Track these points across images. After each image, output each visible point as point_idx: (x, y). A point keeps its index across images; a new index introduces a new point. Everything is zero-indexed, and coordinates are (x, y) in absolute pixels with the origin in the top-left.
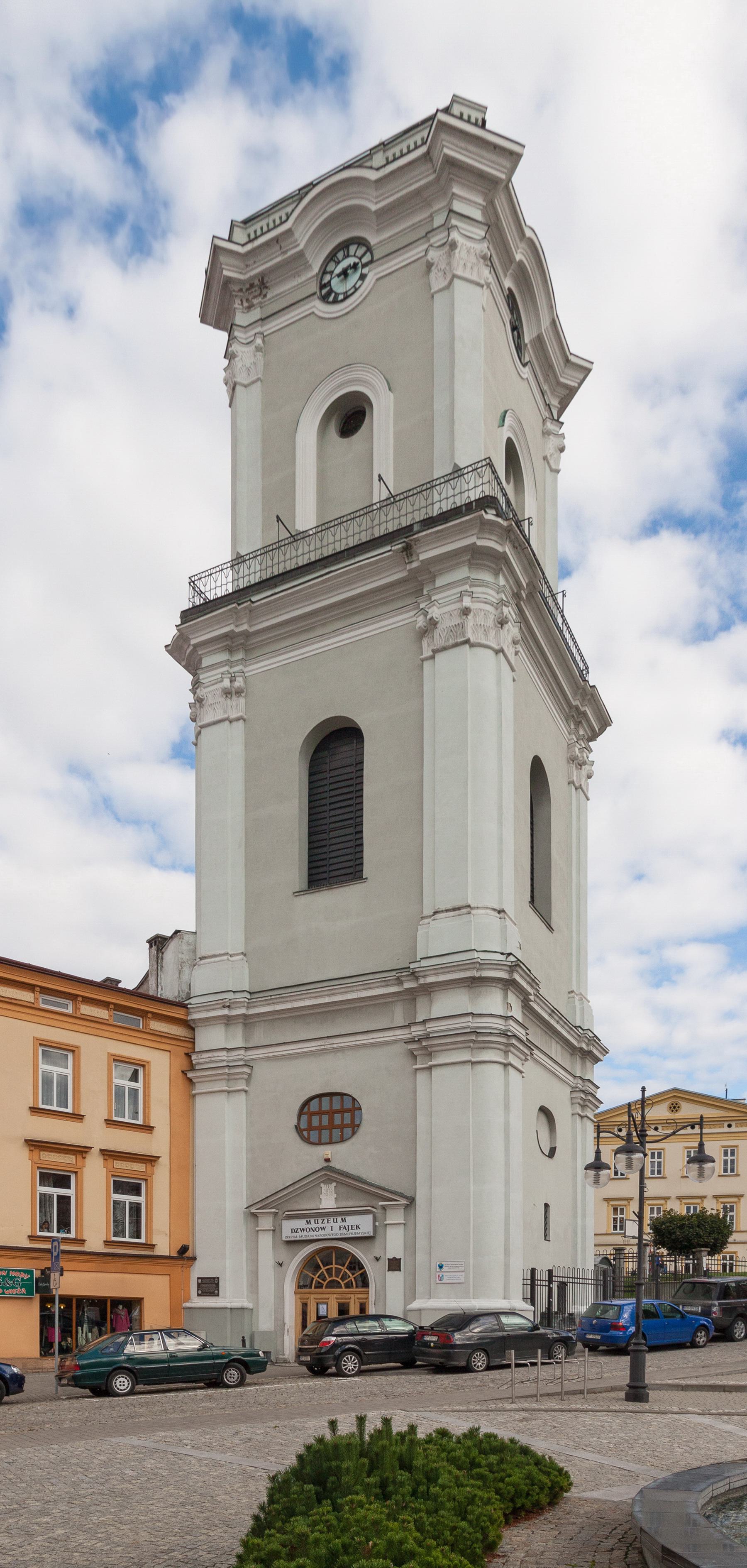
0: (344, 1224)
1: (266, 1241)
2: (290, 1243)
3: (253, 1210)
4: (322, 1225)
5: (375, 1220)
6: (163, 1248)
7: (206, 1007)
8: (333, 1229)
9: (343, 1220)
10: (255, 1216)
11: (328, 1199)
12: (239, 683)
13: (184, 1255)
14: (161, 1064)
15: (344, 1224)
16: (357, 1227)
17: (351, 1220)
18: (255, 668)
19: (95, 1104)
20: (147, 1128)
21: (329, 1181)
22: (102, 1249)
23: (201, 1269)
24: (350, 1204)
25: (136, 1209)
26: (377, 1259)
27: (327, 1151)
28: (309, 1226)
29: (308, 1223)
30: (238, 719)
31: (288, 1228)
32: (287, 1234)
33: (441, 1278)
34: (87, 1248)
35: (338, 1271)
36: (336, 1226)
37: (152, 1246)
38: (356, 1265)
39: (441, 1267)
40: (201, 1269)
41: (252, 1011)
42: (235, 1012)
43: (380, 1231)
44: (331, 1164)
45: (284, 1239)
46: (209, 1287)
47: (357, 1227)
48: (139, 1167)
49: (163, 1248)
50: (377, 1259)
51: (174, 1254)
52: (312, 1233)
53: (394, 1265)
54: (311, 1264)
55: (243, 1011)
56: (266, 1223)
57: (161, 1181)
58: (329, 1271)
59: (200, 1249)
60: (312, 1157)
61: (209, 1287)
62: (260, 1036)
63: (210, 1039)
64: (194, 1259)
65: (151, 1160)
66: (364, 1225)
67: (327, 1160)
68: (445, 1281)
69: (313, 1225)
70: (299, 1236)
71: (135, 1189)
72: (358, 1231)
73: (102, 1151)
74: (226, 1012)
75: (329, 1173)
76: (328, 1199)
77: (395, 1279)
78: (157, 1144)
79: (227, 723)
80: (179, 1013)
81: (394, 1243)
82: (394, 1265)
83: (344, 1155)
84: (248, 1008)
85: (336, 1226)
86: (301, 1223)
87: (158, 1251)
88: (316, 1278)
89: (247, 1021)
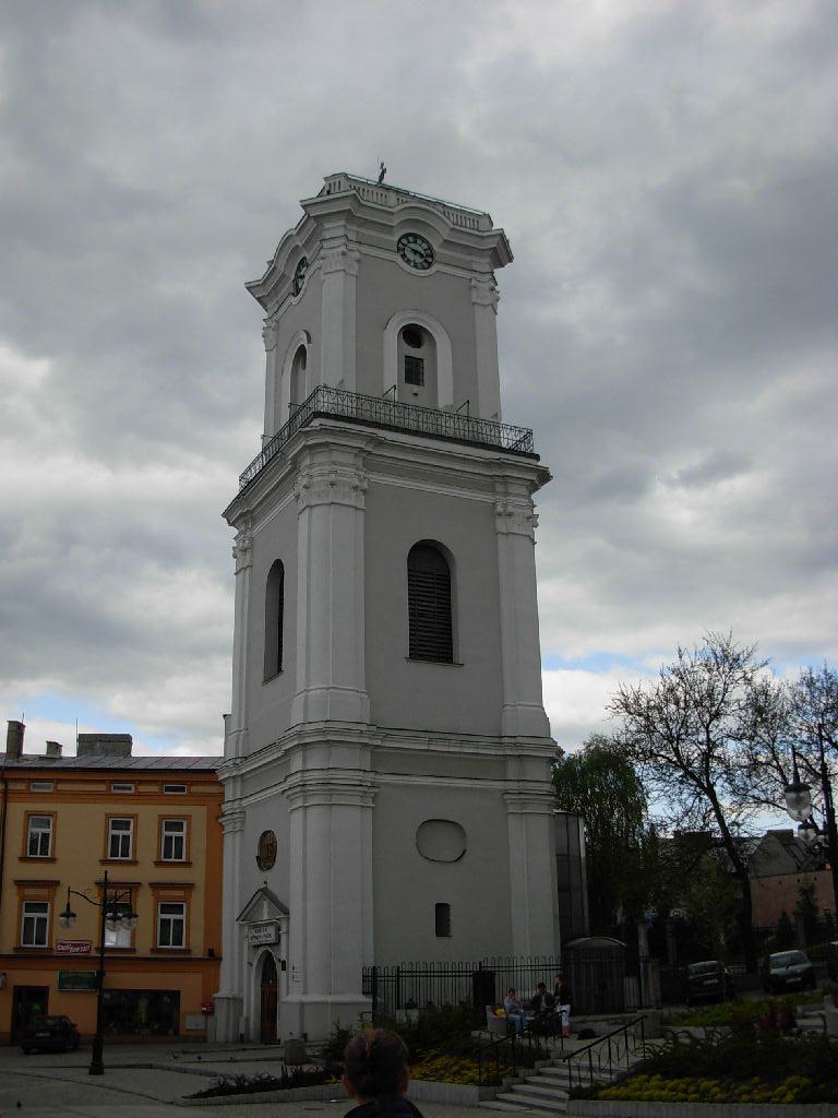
6: (198, 950)
22: (149, 955)
34: (137, 955)
48: (180, 893)
49: (198, 950)
57: (198, 900)
63: (229, 796)
64: (221, 959)
65: (188, 887)
71: (178, 909)
73: (151, 885)
78: (196, 875)
80: (208, 777)
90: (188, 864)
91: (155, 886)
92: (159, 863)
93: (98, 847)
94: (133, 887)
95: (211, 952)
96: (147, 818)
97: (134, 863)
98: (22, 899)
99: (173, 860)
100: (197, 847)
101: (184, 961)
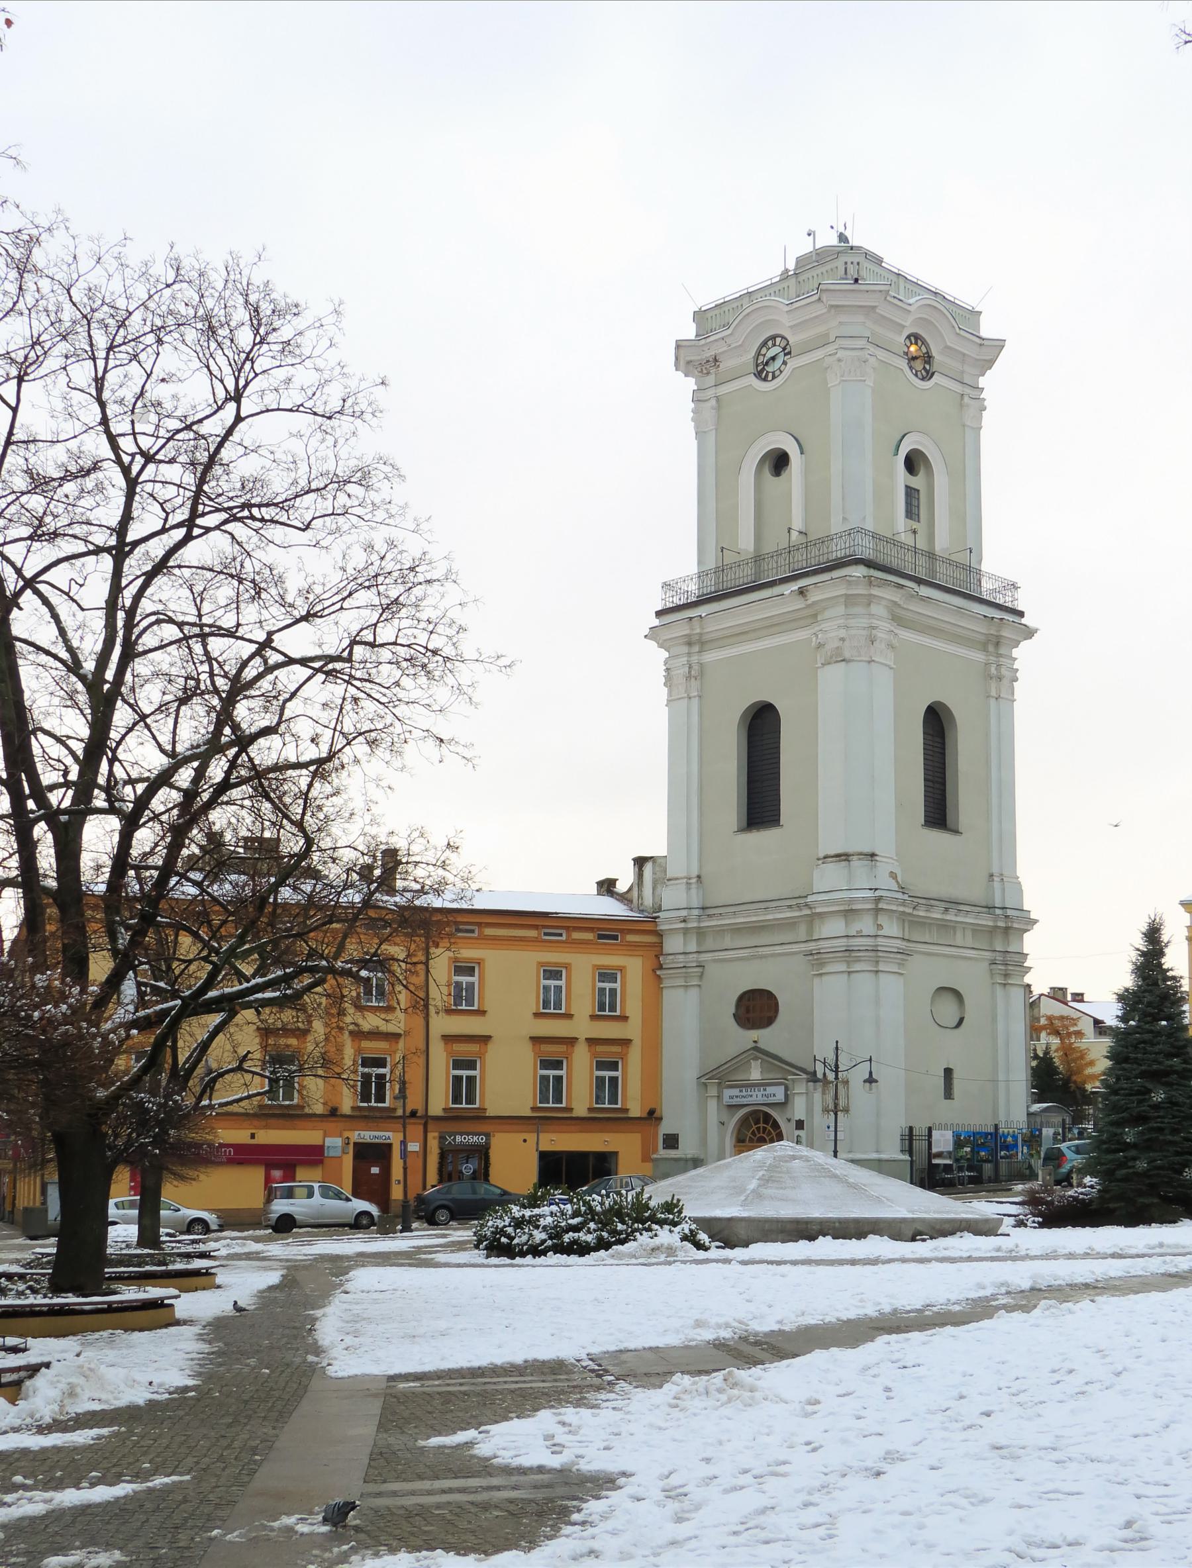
1: (712, 1105)
2: (730, 1106)
3: (703, 1080)
5: (787, 1089)
6: (636, 1111)
7: (669, 920)
8: (757, 1097)
10: (705, 1084)
11: (755, 1073)
13: (653, 1117)
14: (634, 967)
17: (770, 1090)
19: (582, 1000)
20: (624, 1018)
21: (756, 1059)
23: (666, 1128)
24: (771, 1076)
25: (614, 1080)
26: (789, 1120)
27: (754, 1034)
32: (726, 1100)
35: (765, 1129)
36: (760, 1094)
37: (627, 1110)
38: (776, 1125)
40: (666, 1128)
41: (702, 925)
42: (690, 925)
43: (791, 1097)
46: (672, 1141)
48: (616, 1049)
49: (636, 1111)
50: (789, 1120)
51: (645, 1115)
53: (800, 1125)
54: (744, 1123)
55: (695, 925)
56: (713, 1091)
58: (758, 1129)
59: (667, 1111)
61: (672, 1141)
62: (710, 943)
63: (673, 944)
64: (661, 1119)
65: (626, 1042)
66: (779, 1094)
69: (744, 1093)
70: (735, 1101)
73: (589, 1040)
74: (682, 925)
75: (757, 1051)
76: (755, 1073)
78: (632, 1030)
81: (799, 1109)
85: (760, 1094)
86: (736, 1092)
87: (631, 1115)
88: (749, 1134)
89: (701, 933)
90: (624, 1018)
91: (591, 1042)
92: (594, 1017)
93: (532, 1003)
94: (571, 1041)
95: (651, 1112)
96: (583, 966)
97: (568, 1016)
98: (450, 1053)
99: (607, 1013)
100: (633, 1006)
101: (619, 1120)
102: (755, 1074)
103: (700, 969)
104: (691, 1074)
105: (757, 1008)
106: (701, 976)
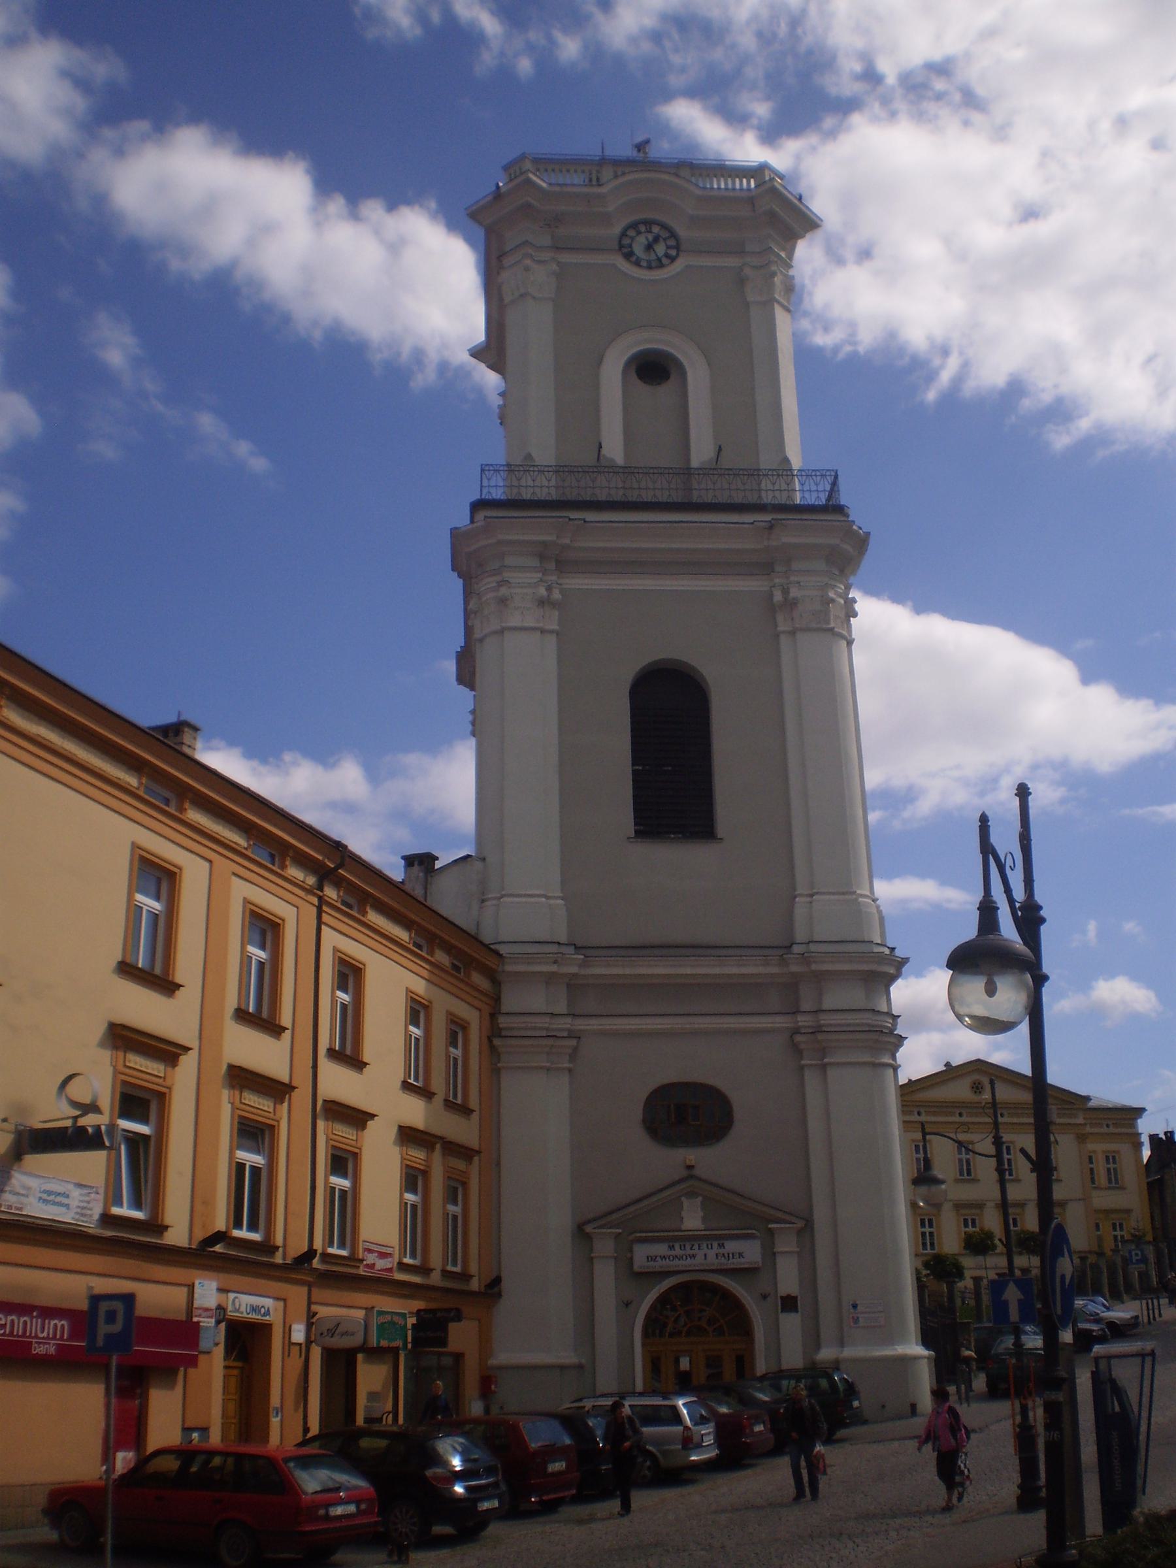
0: (721, 1251)
4: (692, 1252)
8: (706, 1257)
9: (721, 1246)
12: (556, 595)
15: (721, 1251)
16: (741, 1255)
17: (731, 1246)
18: (576, 582)
21: (691, 1194)
27: (691, 1155)
28: (673, 1253)
29: (672, 1248)
30: (552, 632)
31: (641, 1255)
33: (856, 1320)
36: (711, 1254)
39: (855, 1306)
41: (583, 972)
44: (697, 1172)
45: (636, 1268)
47: (741, 1255)
50: (765, 1297)
52: (676, 1262)
53: (789, 1304)
60: (668, 1161)
66: (751, 1252)
67: (690, 1167)
68: (862, 1323)
69: (678, 1251)
70: (659, 1265)
72: (742, 1260)
77: (791, 1324)
79: (539, 633)
82: (789, 1304)
83: (709, 1160)
84: (580, 966)
85: (711, 1254)
86: (661, 1249)
102: (692, 1219)
103: (574, 1042)
104: (559, 1219)
105: (687, 1113)
106: (574, 1055)
